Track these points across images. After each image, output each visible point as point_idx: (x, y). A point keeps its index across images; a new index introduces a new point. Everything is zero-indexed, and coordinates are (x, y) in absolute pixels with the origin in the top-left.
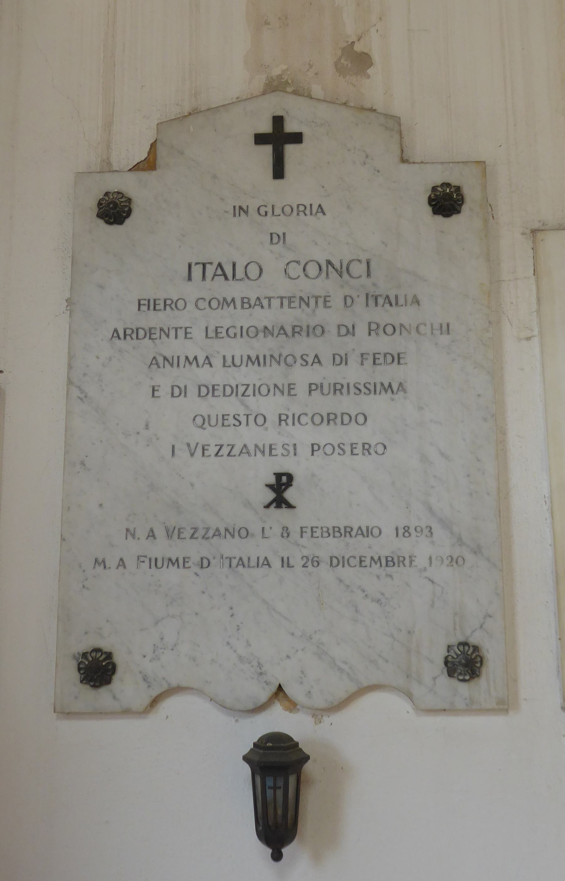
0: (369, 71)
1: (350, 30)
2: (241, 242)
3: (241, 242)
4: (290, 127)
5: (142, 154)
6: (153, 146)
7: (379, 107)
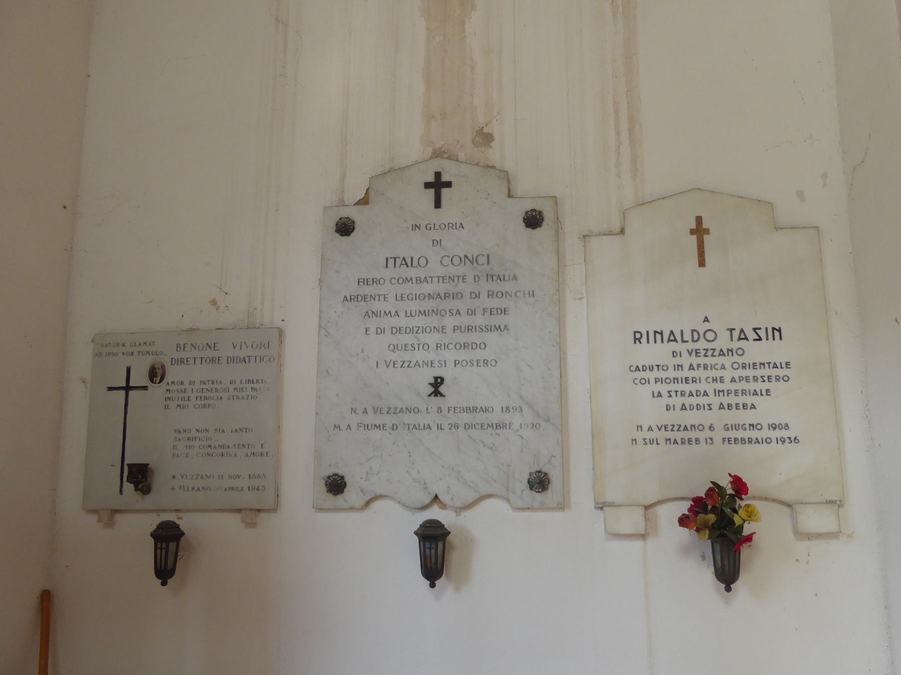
0: (492, 144)
1: (481, 120)
2: (416, 245)
3: (416, 245)
4: (445, 178)
5: (361, 195)
6: (368, 190)
7: (498, 166)
